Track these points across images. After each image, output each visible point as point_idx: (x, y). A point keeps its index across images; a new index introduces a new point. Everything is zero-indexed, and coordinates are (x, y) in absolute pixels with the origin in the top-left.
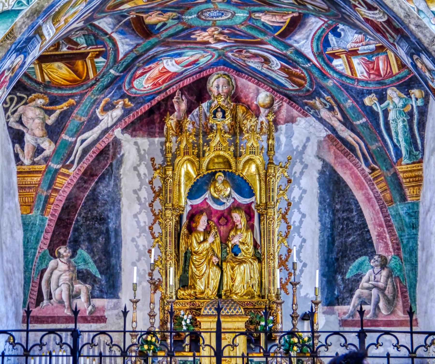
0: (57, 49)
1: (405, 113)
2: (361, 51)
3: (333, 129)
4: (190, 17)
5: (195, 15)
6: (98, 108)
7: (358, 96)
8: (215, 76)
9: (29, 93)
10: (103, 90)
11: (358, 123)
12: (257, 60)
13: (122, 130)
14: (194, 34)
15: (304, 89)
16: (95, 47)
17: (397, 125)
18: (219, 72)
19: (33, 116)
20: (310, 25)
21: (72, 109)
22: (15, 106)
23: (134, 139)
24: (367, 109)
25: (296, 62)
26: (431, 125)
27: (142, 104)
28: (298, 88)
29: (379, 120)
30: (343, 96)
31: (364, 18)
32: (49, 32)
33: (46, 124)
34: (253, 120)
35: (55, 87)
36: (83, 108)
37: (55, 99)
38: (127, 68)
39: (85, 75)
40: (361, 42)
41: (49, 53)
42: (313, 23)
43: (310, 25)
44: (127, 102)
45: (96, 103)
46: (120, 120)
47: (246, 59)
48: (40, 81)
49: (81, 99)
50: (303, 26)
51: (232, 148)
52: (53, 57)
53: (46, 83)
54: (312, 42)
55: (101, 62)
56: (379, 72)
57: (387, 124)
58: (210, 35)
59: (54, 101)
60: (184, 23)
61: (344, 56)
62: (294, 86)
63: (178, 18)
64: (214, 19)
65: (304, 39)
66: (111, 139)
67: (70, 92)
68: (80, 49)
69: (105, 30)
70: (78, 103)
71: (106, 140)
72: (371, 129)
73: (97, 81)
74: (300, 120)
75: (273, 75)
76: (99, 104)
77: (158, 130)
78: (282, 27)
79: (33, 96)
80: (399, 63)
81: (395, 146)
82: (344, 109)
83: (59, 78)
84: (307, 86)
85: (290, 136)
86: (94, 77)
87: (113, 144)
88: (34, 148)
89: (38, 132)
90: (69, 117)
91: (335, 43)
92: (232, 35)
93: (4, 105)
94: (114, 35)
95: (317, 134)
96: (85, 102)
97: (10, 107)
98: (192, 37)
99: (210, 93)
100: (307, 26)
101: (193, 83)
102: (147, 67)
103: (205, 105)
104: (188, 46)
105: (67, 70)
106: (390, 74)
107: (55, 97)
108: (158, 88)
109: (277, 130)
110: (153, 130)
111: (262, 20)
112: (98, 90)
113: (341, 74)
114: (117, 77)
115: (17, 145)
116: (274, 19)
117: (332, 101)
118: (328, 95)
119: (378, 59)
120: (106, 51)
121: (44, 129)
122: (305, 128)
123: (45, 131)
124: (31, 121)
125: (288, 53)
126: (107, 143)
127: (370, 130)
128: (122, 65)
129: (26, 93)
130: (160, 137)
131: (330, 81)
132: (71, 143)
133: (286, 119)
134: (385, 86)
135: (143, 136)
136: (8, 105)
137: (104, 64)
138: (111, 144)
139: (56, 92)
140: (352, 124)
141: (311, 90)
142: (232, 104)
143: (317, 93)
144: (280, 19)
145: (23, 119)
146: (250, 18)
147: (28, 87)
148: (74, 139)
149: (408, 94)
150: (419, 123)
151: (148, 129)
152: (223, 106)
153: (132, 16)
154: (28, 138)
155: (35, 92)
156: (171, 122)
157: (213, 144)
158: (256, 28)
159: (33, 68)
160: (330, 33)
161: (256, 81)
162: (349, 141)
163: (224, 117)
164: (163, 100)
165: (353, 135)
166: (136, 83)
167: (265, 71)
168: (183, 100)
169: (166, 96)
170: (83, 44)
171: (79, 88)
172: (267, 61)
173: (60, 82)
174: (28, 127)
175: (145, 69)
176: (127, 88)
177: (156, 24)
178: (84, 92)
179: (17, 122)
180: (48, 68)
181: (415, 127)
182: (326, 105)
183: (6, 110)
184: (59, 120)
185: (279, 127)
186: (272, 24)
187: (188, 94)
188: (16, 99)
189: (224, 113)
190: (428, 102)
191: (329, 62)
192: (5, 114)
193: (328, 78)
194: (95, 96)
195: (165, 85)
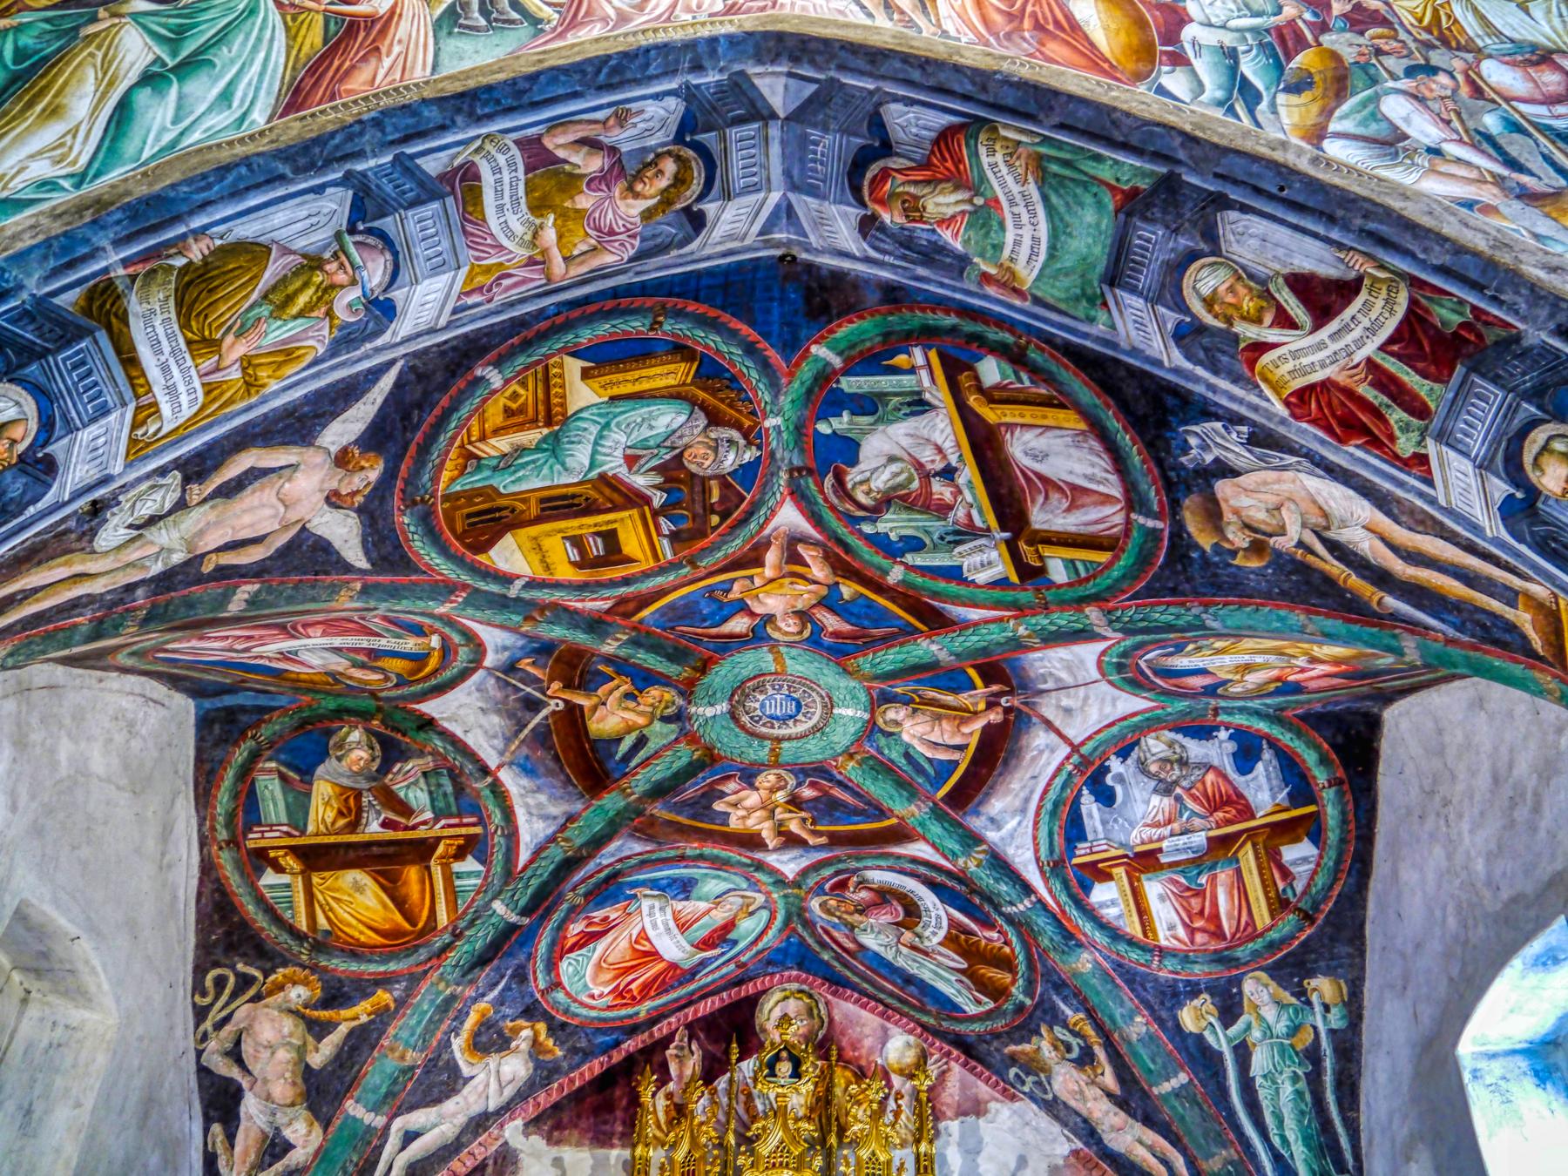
0: (353, 826)
1: (1297, 1054)
2: (1169, 853)
3: (1088, 1132)
4: (709, 712)
6: (457, 1035)
7: (1162, 1003)
8: (778, 996)
9: (268, 965)
10: (472, 968)
11: (1166, 1087)
13: (526, 1125)
14: (723, 795)
15: (1008, 1006)
16: (455, 821)
17: (1277, 1090)
18: (786, 985)
19: (272, 1038)
20: (1034, 759)
21: (382, 1022)
22: (227, 1004)
23: (555, 1151)
24: (1190, 1041)
25: (989, 898)
26: (1382, 1077)
27: (587, 1055)
28: (992, 1005)
29: (1225, 1078)
30: (1122, 1004)
33: (307, 1066)
35: (343, 950)
36: (413, 1022)
37: (339, 989)
38: (541, 903)
39: (425, 913)
40: (1170, 822)
41: (332, 839)
42: (1041, 752)
43: (1034, 759)
44: (542, 1037)
45: (451, 1014)
46: (522, 1096)
47: (857, 917)
48: (304, 929)
49: (409, 993)
50: (1014, 762)
51: (818, 1162)
52: (342, 852)
53: (319, 937)
54: (1036, 823)
55: (469, 874)
56: (1219, 926)
57: (1247, 1086)
59: (336, 995)
60: (693, 739)
61: (1120, 872)
62: (979, 1002)
63: (679, 717)
66: (494, 1148)
67: (382, 969)
68: (414, 828)
69: (483, 756)
70: (401, 1003)
71: (480, 1149)
72: (1205, 1107)
73: (457, 936)
74: (997, 1111)
76: (461, 1016)
77: (620, 1129)
78: (956, 763)
79: (279, 974)
80: (1272, 894)
81: (1277, 1158)
82: (1124, 1049)
83: (354, 922)
84: (1017, 992)
85: (972, 1151)
86: (451, 922)
87: (495, 1163)
88: (264, 1141)
89: (282, 1090)
90: (373, 1048)
91: (1100, 828)
92: (826, 807)
93: (197, 998)
94: (505, 776)
95: (1046, 1149)
96: (420, 1004)
97: (212, 1005)
98: (719, 806)
99: (762, 1037)
100: (1025, 763)
101: (721, 1011)
102: (598, 915)
105: (377, 896)
106: (1250, 929)
107: (340, 981)
108: (630, 1011)
110: (607, 1127)
111: (905, 737)
112: (456, 966)
113: (1115, 934)
114: (512, 928)
115: (216, 1128)
117: (1089, 1031)
118: (1076, 1010)
119: (1213, 879)
120: (486, 836)
121: (299, 1081)
122: (1012, 1131)
123: (302, 1087)
124: (265, 1054)
126: (480, 1158)
127: (1201, 1109)
128: (527, 887)
129: (259, 963)
130: (623, 1146)
131: (1086, 955)
132: (369, 1129)
133: (959, 1106)
134: (1237, 968)
135: (579, 1144)
136: (208, 1000)
137: (479, 882)
138: (491, 1162)
139: (343, 967)
140: (1146, 1095)
141: (1028, 1002)
142: (819, 1063)
143: (1045, 1012)
144: (953, 735)
145: (243, 1046)
146: (871, 729)
147: (269, 945)
148: (380, 1121)
149: (1301, 993)
150: (1339, 1085)
151: (596, 1125)
152: (794, 1046)
154: (251, 1106)
155: (285, 964)
157: (765, 1149)
158: (884, 768)
159: (288, 886)
160: (1085, 791)
161: (881, 1008)
162: (1138, 1160)
163: (796, 1074)
164: (641, 1051)
165: (1151, 1136)
166: (566, 967)
168: (692, 1053)
169: (649, 1042)
170: (422, 811)
171: (407, 956)
172: (912, 912)
173: (356, 934)
174: (255, 1073)
176: (542, 985)
177: (619, 740)
178: (420, 969)
179: (227, 1054)
180: (328, 889)
181: (1330, 1097)
182: (1069, 1049)
183: (201, 1014)
184: (345, 1056)
185: (942, 1125)
187: (707, 1037)
188: (232, 980)
189: (797, 1063)
190: (1360, 1017)
191: (1082, 895)
192: (197, 1026)
193: (1080, 945)
194: (447, 986)
195: (648, 1004)
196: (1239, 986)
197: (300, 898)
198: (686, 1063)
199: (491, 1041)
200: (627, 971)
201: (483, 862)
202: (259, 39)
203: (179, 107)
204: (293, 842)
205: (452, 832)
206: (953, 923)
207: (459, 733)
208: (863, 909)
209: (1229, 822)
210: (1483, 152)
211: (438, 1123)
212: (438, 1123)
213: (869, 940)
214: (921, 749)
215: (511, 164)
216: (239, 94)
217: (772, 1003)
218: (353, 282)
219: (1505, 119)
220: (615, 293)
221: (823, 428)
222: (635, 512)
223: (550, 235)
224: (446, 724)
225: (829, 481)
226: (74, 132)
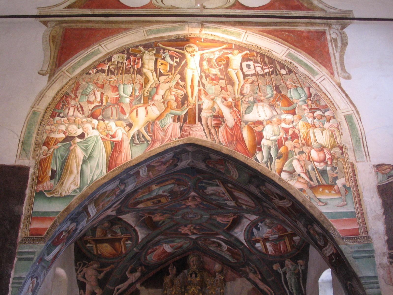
0: (105, 236)
4: (178, 217)
5: (181, 216)
11: (270, 279)
12: (214, 245)
31: (277, 206)
32: (92, 211)
34: (212, 278)
40: (271, 233)
41: (101, 238)
42: (245, 222)
48: (96, 254)
58: (188, 229)
59: (103, 266)
61: (261, 241)
62: (234, 260)
64: (191, 219)
65: (240, 231)
71: (131, 290)
75: (223, 254)
78: (228, 224)
79: (92, 262)
84: (242, 260)
89: (94, 283)
94: (136, 228)
98: (179, 230)
102: (154, 248)
103: (186, 271)
104: (177, 236)
109: (225, 285)
114: (138, 253)
116: (223, 220)
125: (232, 240)
136: (77, 268)
141: (244, 262)
146: (210, 219)
148: (113, 288)
149: (296, 263)
150: (303, 279)
153: (146, 217)
154: (88, 287)
156: (167, 280)
160: (254, 228)
163: (196, 277)
166: (148, 257)
167: (218, 252)
172: (220, 245)
175: (153, 249)
177: (159, 222)
182: (252, 270)
183: (77, 270)
185: (227, 283)
186: (222, 222)
188: (82, 264)
190: (307, 267)
192: (76, 272)
196: (285, 262)
197: (95, 248)
198: (173, 271)
199: (133, 271)
200: (161, 255)
201: (131, 241)
202: (100, 149)
203: (91, 170)
204: (93, 239)
205: (125, 237)
206: (228, 247)
207: (127, 221)
208: (210, 244)
209: (283, 233)
210: (307, 175)
211: (123, 286)
212: (123, 286)
213: (211, 248)
214: (220, 222)
215: (145, 168)
216: (100, 164)
217: (191, 257)
218: (119, 190)
219: (312, 166)
220: (162, 176)
221: (199, 185)
222: (164, 198)
223: (151, 173)
224: (124, 220)
225: (201, 191)
226: (76, 177)
